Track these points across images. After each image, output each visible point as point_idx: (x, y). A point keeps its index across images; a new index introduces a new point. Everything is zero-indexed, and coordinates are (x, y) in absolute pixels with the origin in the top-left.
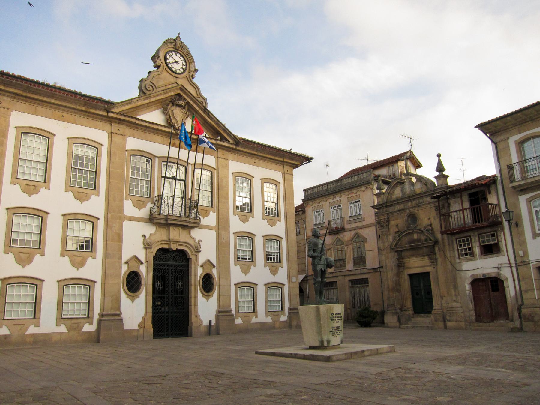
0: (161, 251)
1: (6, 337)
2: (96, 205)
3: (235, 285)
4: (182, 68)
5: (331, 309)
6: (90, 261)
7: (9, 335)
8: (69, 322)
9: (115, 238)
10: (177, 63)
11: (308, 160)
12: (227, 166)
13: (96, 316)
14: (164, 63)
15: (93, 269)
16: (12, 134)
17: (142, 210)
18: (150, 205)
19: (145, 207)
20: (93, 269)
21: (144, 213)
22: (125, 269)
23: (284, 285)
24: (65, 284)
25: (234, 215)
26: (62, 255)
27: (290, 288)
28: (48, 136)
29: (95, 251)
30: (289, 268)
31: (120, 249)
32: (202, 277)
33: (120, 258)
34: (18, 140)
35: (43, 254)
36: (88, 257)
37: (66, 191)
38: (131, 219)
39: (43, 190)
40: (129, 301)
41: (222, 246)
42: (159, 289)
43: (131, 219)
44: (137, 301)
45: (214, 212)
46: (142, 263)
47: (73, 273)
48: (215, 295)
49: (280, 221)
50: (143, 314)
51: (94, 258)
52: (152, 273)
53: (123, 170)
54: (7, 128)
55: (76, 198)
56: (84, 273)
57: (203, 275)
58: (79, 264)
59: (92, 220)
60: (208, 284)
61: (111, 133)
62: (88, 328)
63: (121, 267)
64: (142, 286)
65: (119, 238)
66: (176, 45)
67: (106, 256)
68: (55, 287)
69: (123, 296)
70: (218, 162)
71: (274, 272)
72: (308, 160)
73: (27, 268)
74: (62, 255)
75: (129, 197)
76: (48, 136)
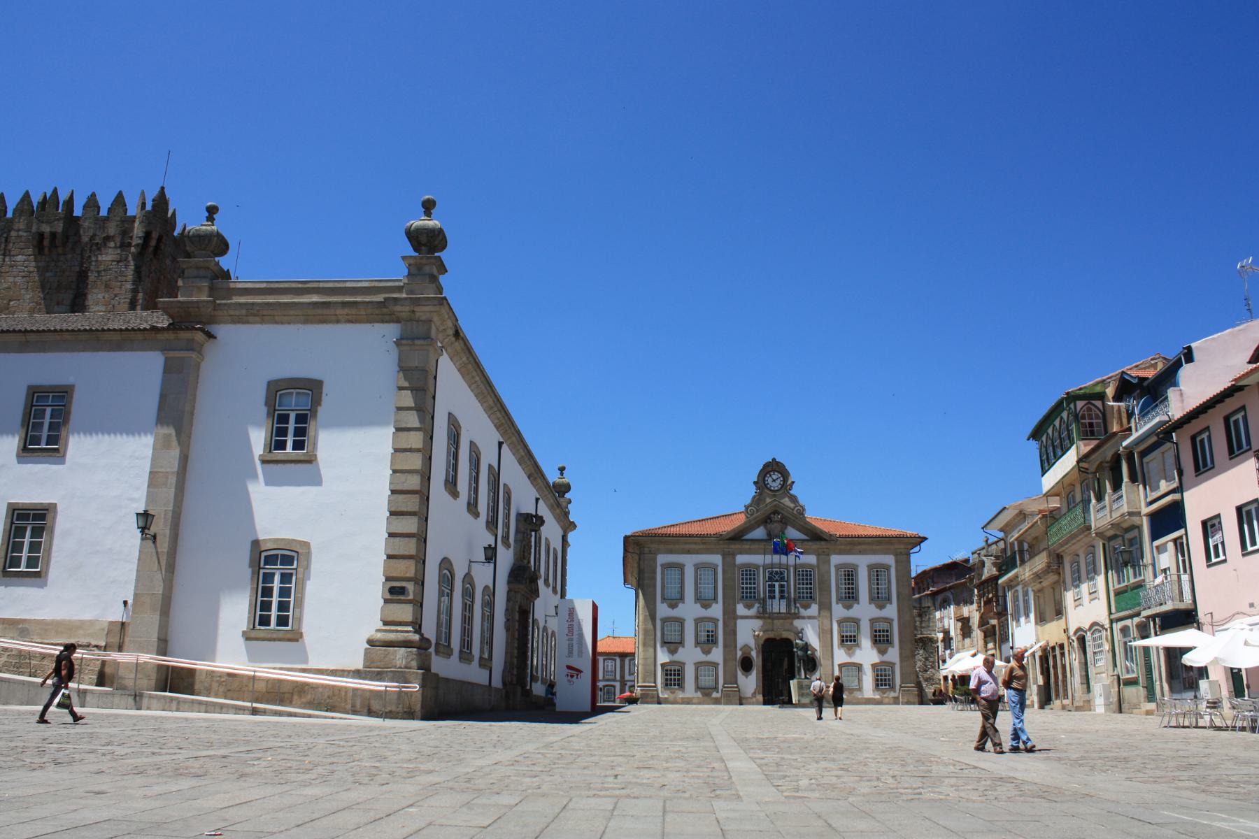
0: (768, 641)
2: (716, 611)
9: (731, 633)
10: (774, 482)
12: (829, 562)
15: (717, 655)
16: (659, 570)
20: (717, 655)
21: (753, 612)
22: (739, 654)
24: (698, 665)
28: (681, 567)
30: (901, 648)
34: (663, 573)
41: (825, 634)
47: (703, 658)
56: (710, 658)
58: (707, 652)
59: (715, 621)
60: (811, 664)
66: (774, 467)
67: (725, 646)
68: (693, 668)
69: (739, 673)
71: (882, 652)
76: (681, 567)
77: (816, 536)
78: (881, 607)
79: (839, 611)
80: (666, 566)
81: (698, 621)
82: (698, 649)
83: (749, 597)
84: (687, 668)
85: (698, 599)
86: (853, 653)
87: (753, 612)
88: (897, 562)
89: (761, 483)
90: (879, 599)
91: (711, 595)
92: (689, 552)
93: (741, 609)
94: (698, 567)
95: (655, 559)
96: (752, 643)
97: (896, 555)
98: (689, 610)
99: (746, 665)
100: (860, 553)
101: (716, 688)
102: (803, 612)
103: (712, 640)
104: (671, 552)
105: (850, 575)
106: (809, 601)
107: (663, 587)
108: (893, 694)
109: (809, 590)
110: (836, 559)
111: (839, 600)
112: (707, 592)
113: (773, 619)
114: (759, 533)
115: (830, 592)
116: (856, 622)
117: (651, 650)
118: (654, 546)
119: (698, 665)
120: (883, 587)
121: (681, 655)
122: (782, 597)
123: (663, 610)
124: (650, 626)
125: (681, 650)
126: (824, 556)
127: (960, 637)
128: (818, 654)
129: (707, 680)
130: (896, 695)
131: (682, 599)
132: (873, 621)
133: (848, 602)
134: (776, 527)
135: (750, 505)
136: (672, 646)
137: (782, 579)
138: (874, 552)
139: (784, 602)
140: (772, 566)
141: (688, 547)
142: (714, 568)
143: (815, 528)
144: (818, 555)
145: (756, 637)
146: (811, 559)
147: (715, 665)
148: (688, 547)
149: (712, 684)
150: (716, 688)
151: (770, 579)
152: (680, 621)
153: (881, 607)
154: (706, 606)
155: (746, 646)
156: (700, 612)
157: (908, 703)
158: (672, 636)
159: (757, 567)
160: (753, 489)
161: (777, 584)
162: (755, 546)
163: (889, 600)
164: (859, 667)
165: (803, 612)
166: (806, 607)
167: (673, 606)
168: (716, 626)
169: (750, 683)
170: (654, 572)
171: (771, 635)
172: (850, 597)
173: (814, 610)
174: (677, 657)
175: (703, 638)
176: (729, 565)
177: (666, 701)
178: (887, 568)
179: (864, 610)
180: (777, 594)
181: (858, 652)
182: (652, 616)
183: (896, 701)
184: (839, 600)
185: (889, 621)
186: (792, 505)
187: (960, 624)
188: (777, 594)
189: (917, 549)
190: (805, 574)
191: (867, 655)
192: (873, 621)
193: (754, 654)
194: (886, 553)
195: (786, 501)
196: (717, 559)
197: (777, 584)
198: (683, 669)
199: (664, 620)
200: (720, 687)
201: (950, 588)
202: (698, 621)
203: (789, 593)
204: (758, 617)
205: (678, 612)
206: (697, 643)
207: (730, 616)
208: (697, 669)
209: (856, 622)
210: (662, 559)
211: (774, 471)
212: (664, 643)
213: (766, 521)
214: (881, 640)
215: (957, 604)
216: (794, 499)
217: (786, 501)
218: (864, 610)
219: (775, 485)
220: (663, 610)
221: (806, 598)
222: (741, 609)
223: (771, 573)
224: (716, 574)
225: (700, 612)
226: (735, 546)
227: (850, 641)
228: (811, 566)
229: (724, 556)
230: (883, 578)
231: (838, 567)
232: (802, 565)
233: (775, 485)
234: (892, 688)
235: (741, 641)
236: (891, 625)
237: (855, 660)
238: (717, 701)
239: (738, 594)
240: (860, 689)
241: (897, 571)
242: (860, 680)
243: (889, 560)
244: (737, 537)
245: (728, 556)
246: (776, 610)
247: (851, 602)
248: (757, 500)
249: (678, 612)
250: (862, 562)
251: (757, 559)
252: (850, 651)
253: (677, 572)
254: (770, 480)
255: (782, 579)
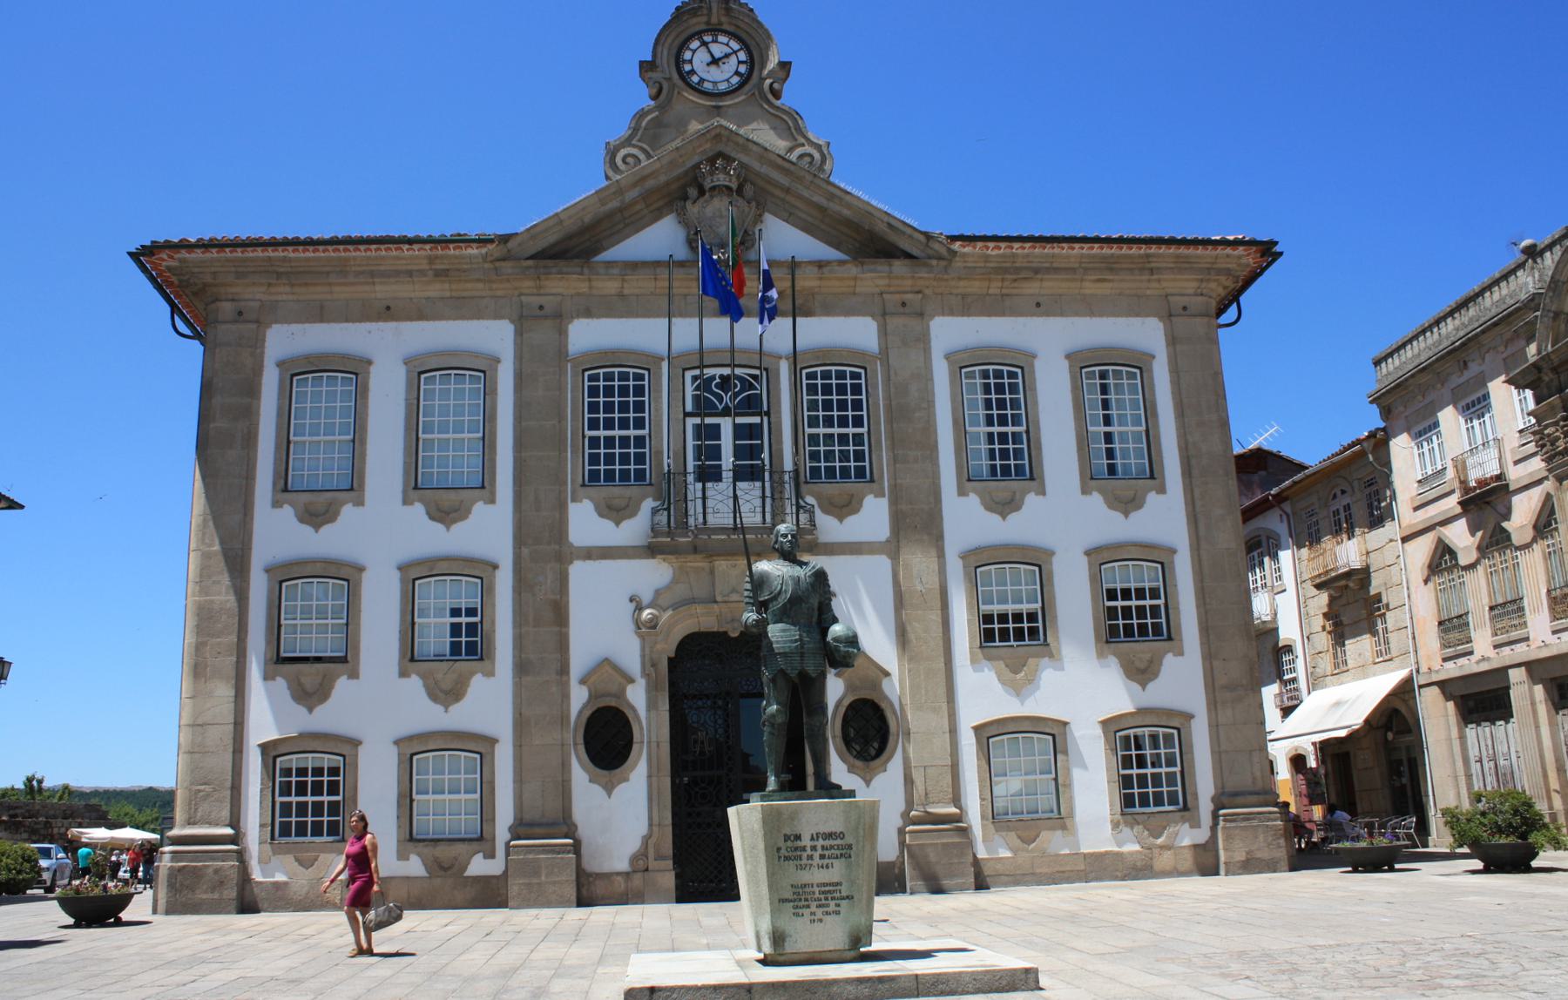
1: (277, 885)
2: (489, 530)
3: (978, 729)
4: (737, 73)
5: (794, 815)
6: (478, 684)
7: (286, 884)
8: (428, 850)
9: (547, 616)
11: (1268, 252)
12: (924, 340)
13: (502, 833)
14: (675, 76)
15: (489, 702)
17: (627, 525)
18: (648, 504)
19: (633, 514)
20: (489, 702)
22: (579, 697)
23: (1190, 717)
24: (412, 749)
25: (962, 492)
26: (403, 674)
27: (1214, 727)
28: (355, 370)
29: (491, 657)
30: (1209, 657)
31: (562, 645)
32: (842, 710)
33: (564, 670)
35: (354, 675)
36: (472, 674)
37: (406, 501)
38: (591, 554)
39: (348, 511)
40: (597, 790)
42: (702, 753)
43: (591, 554)
44: (621, 790)
45: (880, 494)
46: (632, 681)
47: (434, 717)
48: (895, 766)
49: (1162, 490)
50: (643, 829)
51: (490, 673)
52: (667, 707)
53: (561, 417)
54: (258, 370)
55: (432, 518)
57: (846, 703)
59: (480, 570)
60: (870, 730)
61: (521, 317)
62: (479, 866)
63: (566, 696)
64: (635, 747)
65: (559, 614)
67: (522, 667)
69: (580, 774)
70: (883, 332)
71: (1141, 673)
72: (1268, 252)
73: (319, 710)
74: (403, 674)
75: (582, 491)
76: (355, 370)
77: (871, 241)
78: (1128, 505)
79: (967, 520)
80: (298, 370)
81: (415, 573)
82: (415, 683)
83: (616, 471)
84: (365, 757)
85: (415, 486)
86: (1032, 680)
87: (634, 530)
88: (1172, 340)
89: (665, 70)
90: (1115, 473)
91: (466, 466)
92: (388, 313)
93: (585, 522)
94: (421, 370)
95: (258, 344)
96: (630, 654)
97: (1168, 316)
98: (382, 531)
99: (607, 740)
100: (1039, 308)
101: (482, 840)
102: (829, 528)
103: (470, 643)
104: (320, 314)
105: (1002, 387)
106: (852, 486)
107: (284, 446)
108: (1188, 836)
109: (848, 431)
110: (950, 333)
111: (967, 479)
112: (453, 457)
113: (711, 553)
114: (661, 238)
115: (934, 448)
116: (1037, 560)
117: (225, 691)
118: (253, 294)
119: (412, 749)
120: (1127, 429)
121: (346, 707)
122: (740, 474)
123: (277, 533)
124: (224, 597)
125: (342, 685)
126: (903, 318)
127: (1323, 641)
128: (895, 688)
129: (447, 808)
130: (1202, 835)
131: (354, 487)
132: (1100, 556)
133: (1003, 488)
134: (718, 212)
135: (627, 142)
136: (309, 672)
137: (751, 405)
138: (1090, 307)
139: (750, 493)
140: (701, 358)
141: (384, 291)
142: (482, 370)
143: (868, 212)
144: (882, 315)
145: (647, 630)
146: (856, 332)
147: (482, 746)
148: (384, 291)
149: (467, 823)
150: (482, 840)
151: (703, 407)
152: (344, 575)
153: (1128, 505)
154: (446, 515)
155: (607, 671)
156: (425, 536)
157: (1250, 865)
158: (312, 634)
159: (647, 362)
160: (640, 96)
161: (726, 425)
162: (639, 284)
163: (1153, 474)
164: (1055, 734)
165: (829, 528)
166: (844, 508)
167: (316, 516)
168: (487, 590)
169: (622, 814)
170: (252, 390)
171: (704, 620)
172: (1009, 466)
173: (873, 517)
174: (326, 718)
175: (435, 632)
176: (541, 355)
177: (281, 899)
178: (1139, 364)
179: (1065, 517)
180: (728, 460)
181: (1049, 676)
182: (236, 559)
183: (1206, 863)
184: (967, 479)
185: (1160, 556)
186: (779, 144)
187: (1323, 598)
188: (728, 460)
189: (1231, 313)
190: (836, 389)
191: (1084, 689)
192: (1100, 556)
193: (636, 696)
194: (1135, 307)
195: (764, 134)
196: (494, 337)
197: (726, 425)
198: (351, 763)
199: (285, 574)
200: (502, 833)
201: (1280, 499)
202: (415, 573)
203: (776, 455)
204: (651, 551)
205: (338, 539)
206: (410, 657)
207: (544, 551)
208: (407, 765)
209: (1037, 560)
210: (284, 341)
211: (716, 31)
212: (279, 660)
213: (680, 192)
214: (1132, 625)
215: (1308, 536)
216: (790, 124)
217: (764, 134)
218: (1065, 517)
219: (722, 76)
220: (277, 533)
221: (840, 470)
222: (585, 522)
223: (704, 384)
224: (489, 392)
225: (425, 536)
226: (563, 285)
227: (1015, 633)
228: (858, 357)
229: (523, 321)
230: (1125, 398)
231: (961, 363)
232: (825, 355)
233: (722, 76)
234: (1186, 808)
235: (584, 649)
236: (1166, 568)
237: (1040, 704)
238: (490, 895)
239: (574, 466)
240: (1060, 818)
241: (1175, 371)
242: (1060, 787)
243: (1145, 334)
244: (574, 246)
245: (539, 325)
246: (720, 515)
247: (1014, 485)
248: (648, 130)
249: (338, 539)
250: (1049, 343)
251: (641, 334)
252: (1018, 678)
253: (341, 387)
254: (698, 59)
255: (751, 405)
